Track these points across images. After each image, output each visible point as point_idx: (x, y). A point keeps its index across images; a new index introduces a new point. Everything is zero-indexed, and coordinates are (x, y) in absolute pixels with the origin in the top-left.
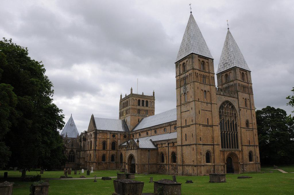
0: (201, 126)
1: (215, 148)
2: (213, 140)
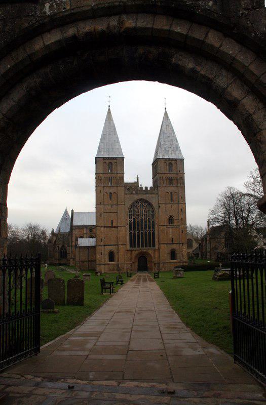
0: (102, 228)
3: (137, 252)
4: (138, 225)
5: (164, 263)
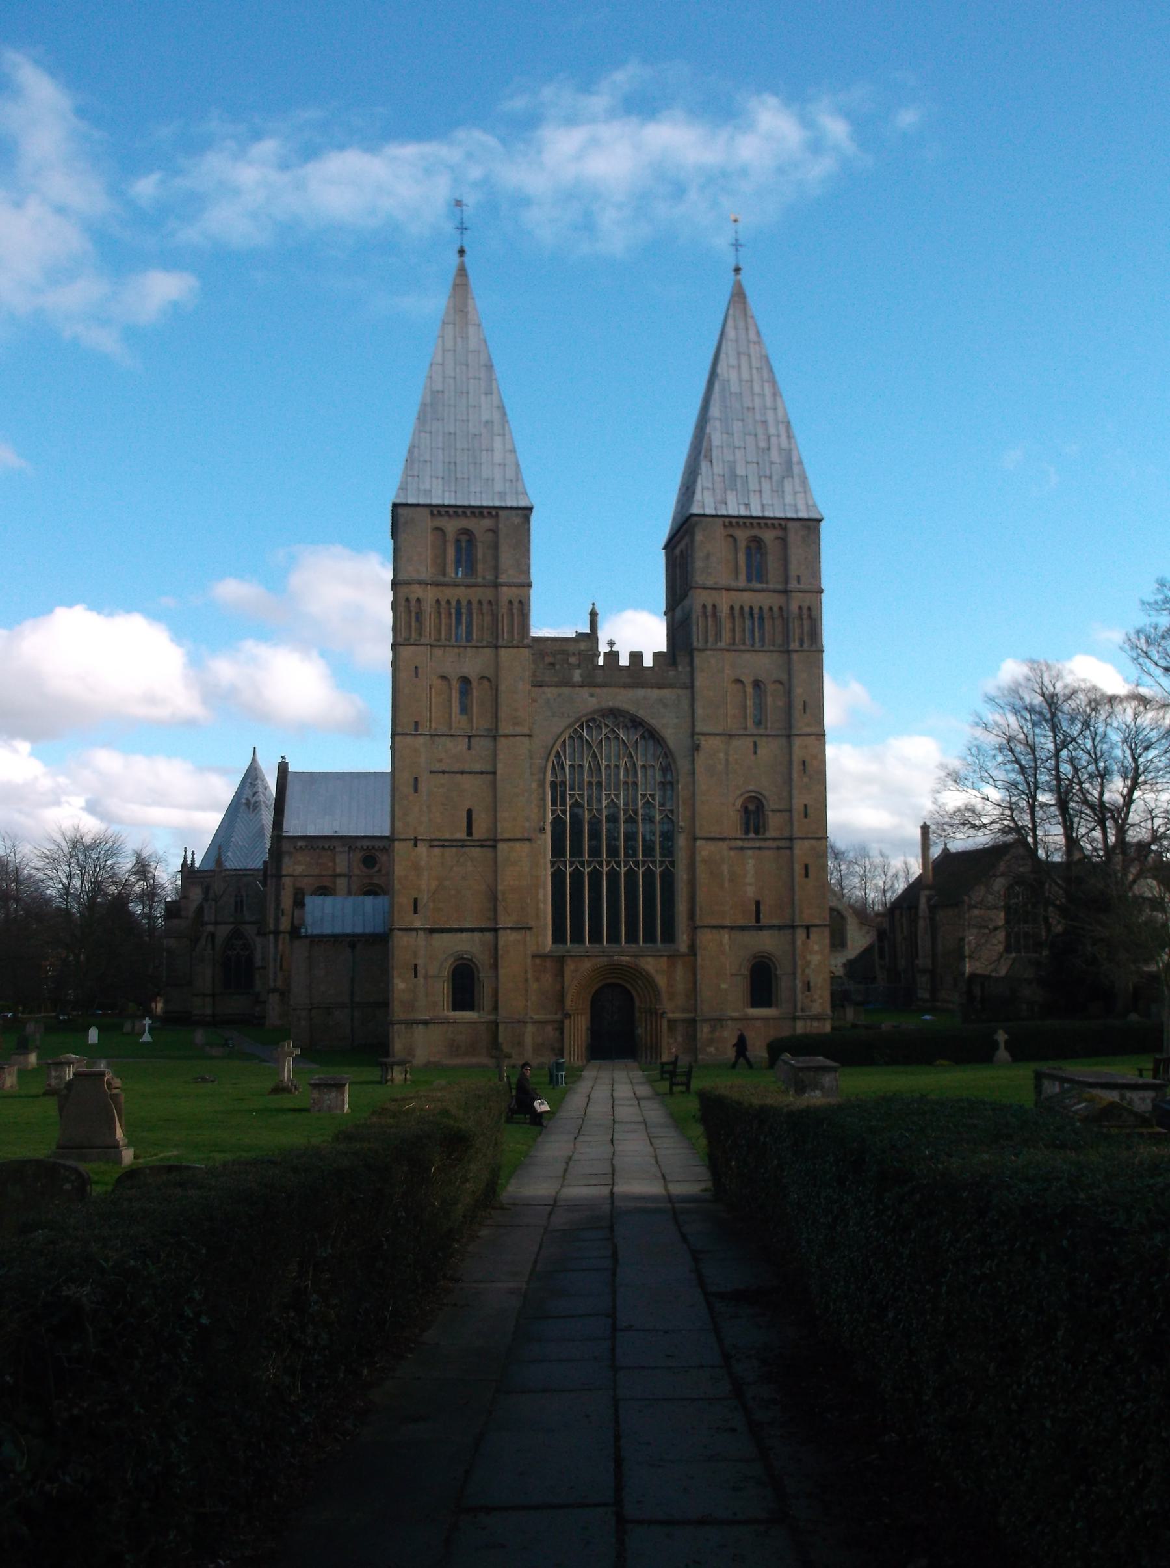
0: (422, 849)
1: (501, 943)
2: (495, 910)
3: (587, 965)
4: (595, 835)
5: (718, 1022)
